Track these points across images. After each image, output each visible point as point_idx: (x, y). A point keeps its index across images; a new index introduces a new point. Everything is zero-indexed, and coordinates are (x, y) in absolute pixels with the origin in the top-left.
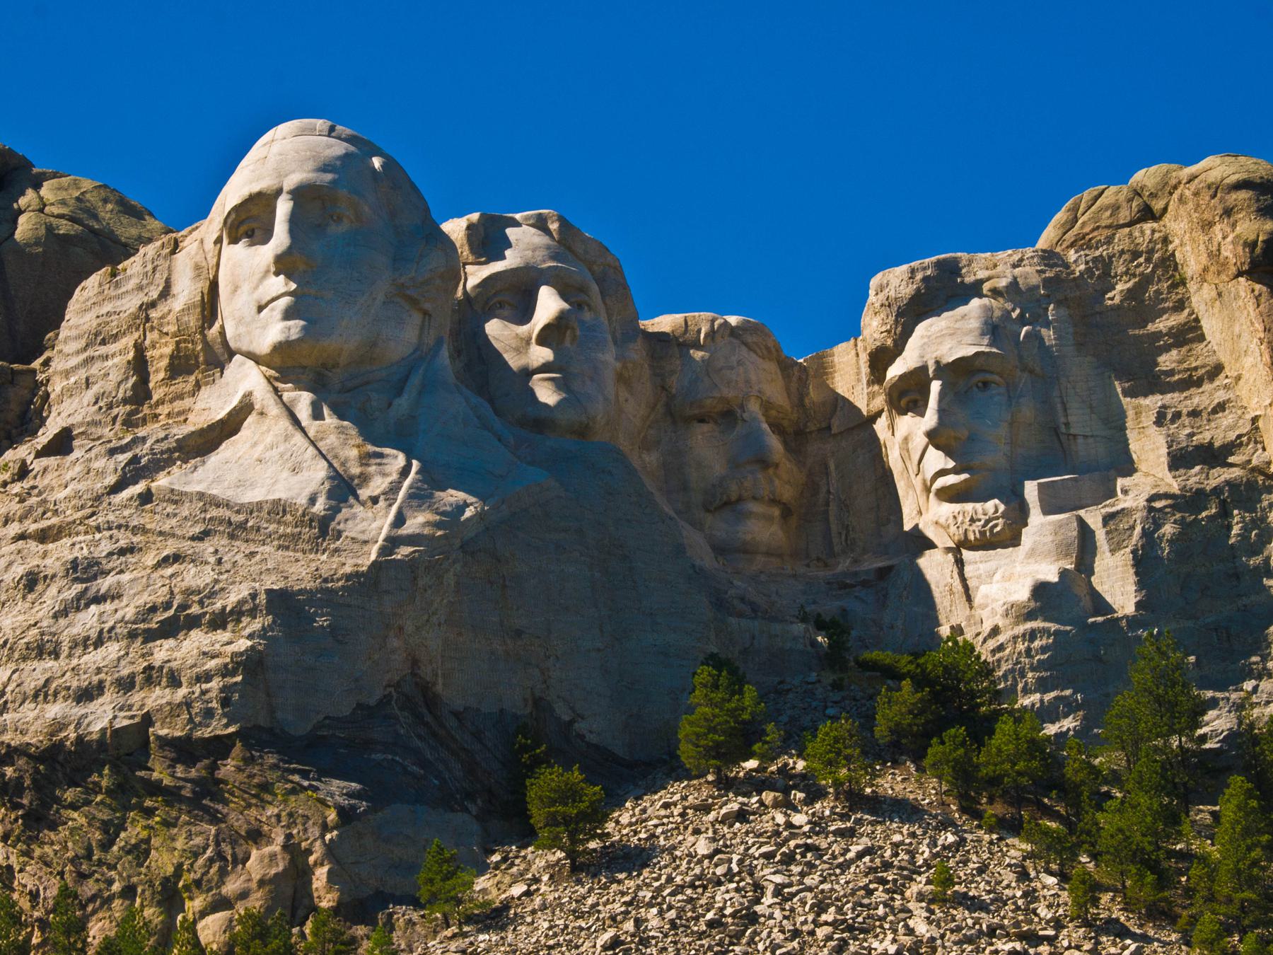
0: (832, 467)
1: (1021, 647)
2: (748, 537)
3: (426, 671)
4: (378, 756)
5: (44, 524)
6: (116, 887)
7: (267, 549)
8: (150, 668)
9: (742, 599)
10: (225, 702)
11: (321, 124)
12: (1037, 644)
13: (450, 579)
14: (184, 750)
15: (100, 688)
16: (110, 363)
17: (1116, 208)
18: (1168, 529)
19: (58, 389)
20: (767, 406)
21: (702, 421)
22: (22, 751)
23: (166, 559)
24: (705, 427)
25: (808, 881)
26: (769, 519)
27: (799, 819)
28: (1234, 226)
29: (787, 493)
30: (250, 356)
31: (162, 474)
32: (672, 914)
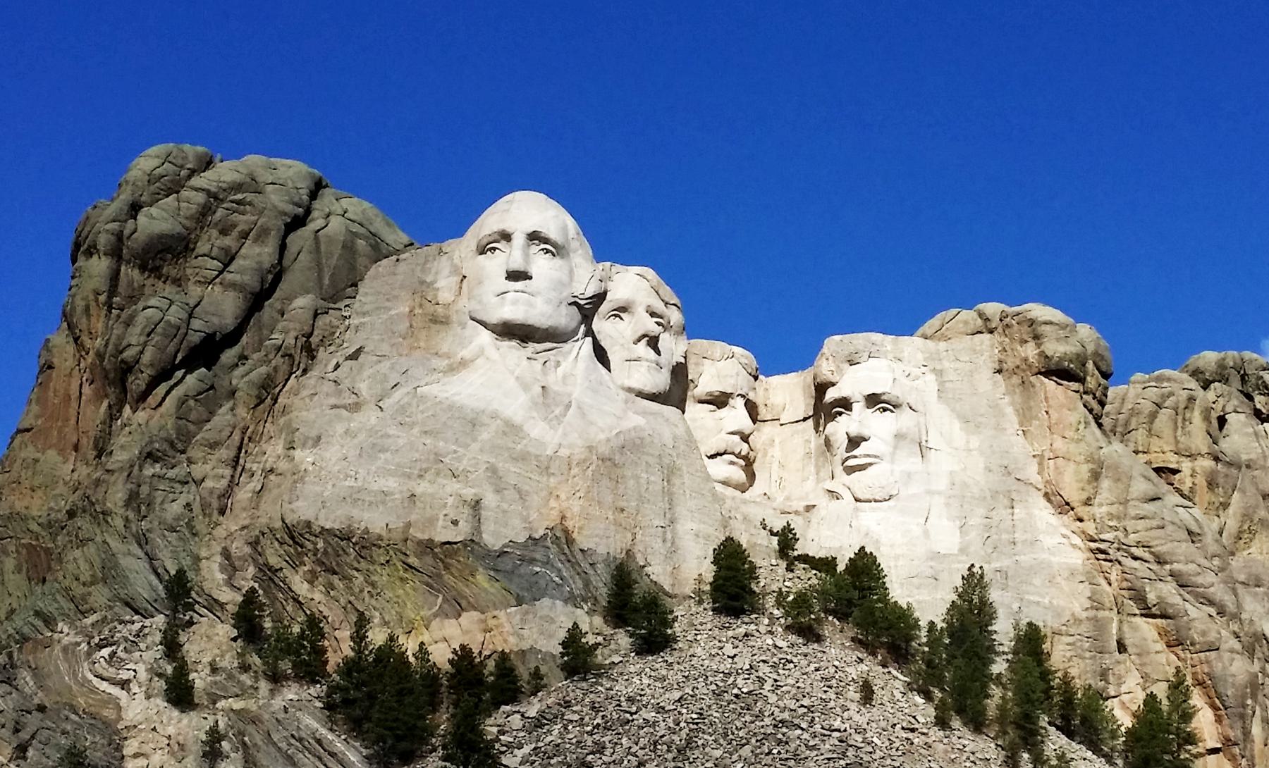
0: (777, 441)
1: (892, 564)
3: (569, 524)
4: (538, 569)
5: (350, 401)
6: (376, 621)
7: (485, 436)
8: (413, 495)
13: (589, 472)
14: (428, 547)
15: (384, 503)
16: (393, 312)
22: (330, 532)
23: (426, 432)
25: (791, 681)
27: (780, 643)
31: (423, 383)
32: (714, 687)
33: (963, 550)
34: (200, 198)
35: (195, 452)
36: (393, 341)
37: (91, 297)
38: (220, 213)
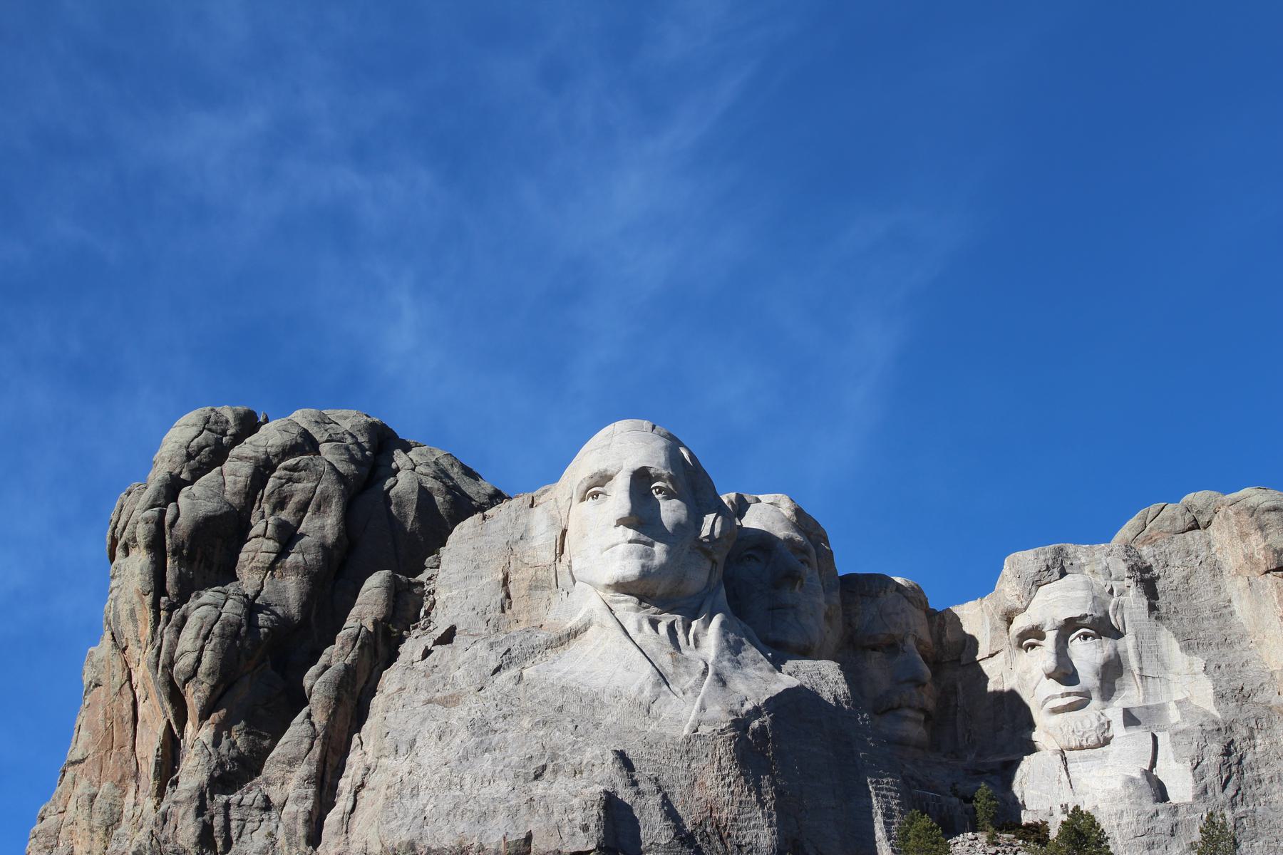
0: (960, 687)
2: (905, 734)
9: (912, 778)
10: (585, 828)
11: (646, 424)
12: (1125, 821)
17: (1173, 519)
18: (1216, 747)
19: (443, 597)
20: (919, 642)
21: (874, 649)
24: (877, 654)
26: (917, 721)
28: (1265, 538)
29: (931, 705)
30: (590, 583)
33: (1196, 797)
34: (246, 469)
35: (271, 769)
36: (488, 616)
37: (136, 599)
38: (271, 483)
